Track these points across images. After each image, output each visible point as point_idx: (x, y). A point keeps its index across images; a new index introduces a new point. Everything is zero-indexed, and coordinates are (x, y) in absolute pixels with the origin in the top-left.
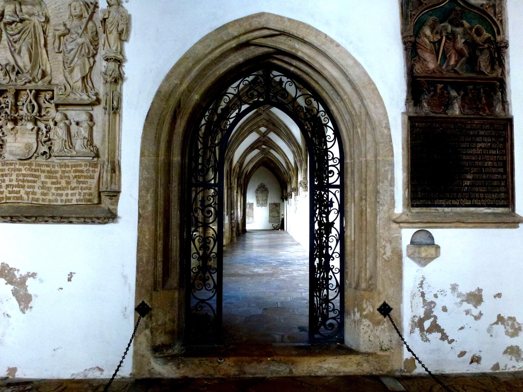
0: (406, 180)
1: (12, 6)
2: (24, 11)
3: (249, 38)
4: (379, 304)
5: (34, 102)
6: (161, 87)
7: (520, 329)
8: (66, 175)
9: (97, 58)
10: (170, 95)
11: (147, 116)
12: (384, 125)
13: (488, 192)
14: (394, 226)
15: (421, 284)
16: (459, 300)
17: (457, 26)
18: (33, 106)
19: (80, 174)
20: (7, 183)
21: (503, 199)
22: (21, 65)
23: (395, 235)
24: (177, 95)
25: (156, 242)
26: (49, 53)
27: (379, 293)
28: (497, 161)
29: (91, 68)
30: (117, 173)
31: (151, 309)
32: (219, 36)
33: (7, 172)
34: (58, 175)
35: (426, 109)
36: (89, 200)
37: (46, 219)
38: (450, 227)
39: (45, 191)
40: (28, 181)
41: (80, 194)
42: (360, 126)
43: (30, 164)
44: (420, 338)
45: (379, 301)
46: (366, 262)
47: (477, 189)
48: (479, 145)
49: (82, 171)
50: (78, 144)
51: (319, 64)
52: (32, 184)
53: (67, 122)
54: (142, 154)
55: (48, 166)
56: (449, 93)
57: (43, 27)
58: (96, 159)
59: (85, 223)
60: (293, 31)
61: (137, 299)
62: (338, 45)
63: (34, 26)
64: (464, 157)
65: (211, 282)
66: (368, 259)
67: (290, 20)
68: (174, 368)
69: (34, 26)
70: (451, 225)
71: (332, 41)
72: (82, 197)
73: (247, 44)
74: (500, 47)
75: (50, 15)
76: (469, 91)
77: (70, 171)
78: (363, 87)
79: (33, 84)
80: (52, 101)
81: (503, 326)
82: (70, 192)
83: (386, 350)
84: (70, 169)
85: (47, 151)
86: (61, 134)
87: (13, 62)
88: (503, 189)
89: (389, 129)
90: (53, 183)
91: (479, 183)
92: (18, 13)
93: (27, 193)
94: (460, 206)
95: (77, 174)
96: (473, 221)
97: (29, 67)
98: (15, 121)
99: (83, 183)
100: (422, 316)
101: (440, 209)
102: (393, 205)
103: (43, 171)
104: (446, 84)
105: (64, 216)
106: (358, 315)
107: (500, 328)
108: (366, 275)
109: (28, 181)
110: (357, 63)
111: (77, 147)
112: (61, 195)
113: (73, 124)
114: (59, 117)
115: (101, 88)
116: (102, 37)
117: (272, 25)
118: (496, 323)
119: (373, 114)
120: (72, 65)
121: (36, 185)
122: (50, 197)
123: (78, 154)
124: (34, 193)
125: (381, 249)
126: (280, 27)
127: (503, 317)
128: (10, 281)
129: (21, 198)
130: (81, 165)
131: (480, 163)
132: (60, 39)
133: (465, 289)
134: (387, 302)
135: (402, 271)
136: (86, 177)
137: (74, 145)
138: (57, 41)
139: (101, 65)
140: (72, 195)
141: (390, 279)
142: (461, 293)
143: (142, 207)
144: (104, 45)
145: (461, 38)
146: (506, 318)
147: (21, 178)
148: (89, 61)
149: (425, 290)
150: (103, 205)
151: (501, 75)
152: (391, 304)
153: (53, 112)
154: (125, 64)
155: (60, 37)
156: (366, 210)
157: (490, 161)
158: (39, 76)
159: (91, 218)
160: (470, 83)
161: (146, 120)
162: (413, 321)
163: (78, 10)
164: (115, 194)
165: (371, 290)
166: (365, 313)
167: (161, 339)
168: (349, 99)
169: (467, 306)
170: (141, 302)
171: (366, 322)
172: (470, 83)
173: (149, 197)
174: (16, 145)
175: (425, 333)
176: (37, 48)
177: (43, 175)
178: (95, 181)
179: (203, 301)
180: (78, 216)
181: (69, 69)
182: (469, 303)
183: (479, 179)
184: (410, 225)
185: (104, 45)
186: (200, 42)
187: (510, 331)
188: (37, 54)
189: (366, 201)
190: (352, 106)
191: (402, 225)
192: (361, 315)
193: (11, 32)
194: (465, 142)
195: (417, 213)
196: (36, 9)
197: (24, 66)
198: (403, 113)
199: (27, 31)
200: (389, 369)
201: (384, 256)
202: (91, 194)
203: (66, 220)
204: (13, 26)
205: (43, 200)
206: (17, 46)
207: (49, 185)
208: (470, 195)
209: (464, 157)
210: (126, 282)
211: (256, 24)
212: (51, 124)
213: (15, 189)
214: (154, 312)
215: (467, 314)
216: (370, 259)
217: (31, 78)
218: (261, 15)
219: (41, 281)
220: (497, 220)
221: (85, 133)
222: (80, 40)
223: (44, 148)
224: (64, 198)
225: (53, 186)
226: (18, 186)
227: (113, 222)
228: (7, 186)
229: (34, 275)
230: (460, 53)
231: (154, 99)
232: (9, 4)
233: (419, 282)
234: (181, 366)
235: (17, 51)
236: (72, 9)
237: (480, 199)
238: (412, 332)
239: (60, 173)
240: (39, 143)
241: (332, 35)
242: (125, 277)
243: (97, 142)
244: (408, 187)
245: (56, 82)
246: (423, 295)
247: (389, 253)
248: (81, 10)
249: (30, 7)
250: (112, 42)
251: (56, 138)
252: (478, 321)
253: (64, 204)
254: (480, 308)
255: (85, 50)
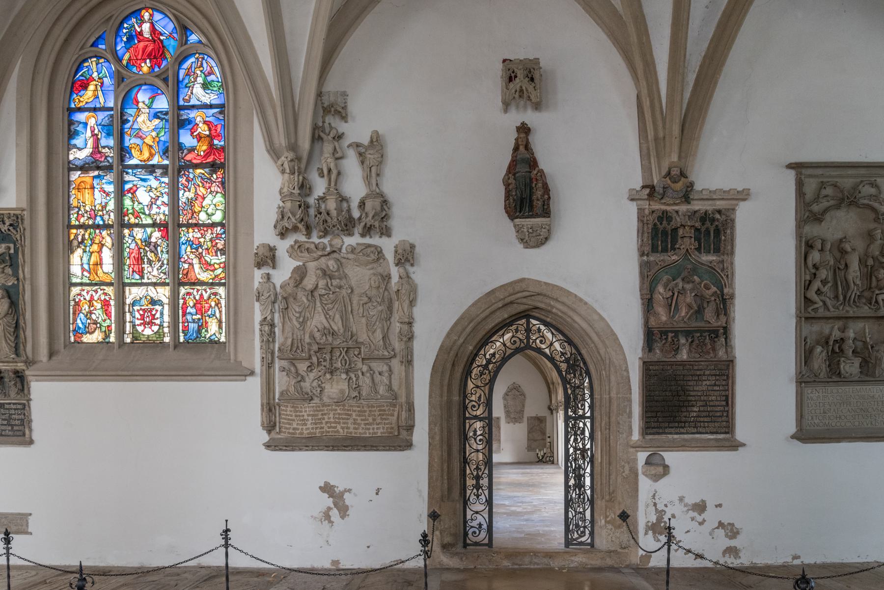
0: (641, 413)
1: (325, 281)
2: (334, 284)
3: (512, 299)
4: (618, 512)
5: (346, 357)
6: (443, 342)
7: (738, 533)
8: (372, 413)
9: (392, 320)
10: (451, 349)
11: (433, 366)
12: (624, 369)
13: (711, 422)
14: (632, 450)
15: (654, 495)
16: (686, 509)
17: (688, 282)
18: (346, 360)
19: (383, 413)
20: (327, 420)
21: (725, 427)
22: (336, 328)
23: (632, 457)
24: (455, 348)
25: (442, 464)
26: (354, 317)
27: (619, 503)
28: (720, 396)
29: (388, 328)
30: (412, 411)
31: (439, 516)
32: (488, 299)
33: (326, 412)
34: (367, 414)
35: (658, 355)
36: (391, 433)
37: (359, 448)
38: (679, 451)
39: (357, 426)
40: (343, 419)
41: (383, 428)
42: (605, 369)
43: (344, 405)
44: (653, 539)
45: (619, 509)
46: (609, 479)
47: (702, 419)
48: (704, 383)
49: (384, 410)
50: (382, 390)
51: (571, 318)
52: (346, 421)
53: (371, 372)
54: (430, 396)
55: (358, 407)
56: (678, 340)
57: (349, 296)
58: (394, 401)
59: (389, 450)
60: (549, 293)
61: (429, 508)
62: (586, 303)
63: (343, 297)
64: (692, 393)
65: (483, 497)
66: (611, 477)
67: (546, 283)
68: (458, 560)
69: (343, 297)
70: (679, 449)
71: (581, 300)
72: (385, 431)
73: (512, 303)
74: (726, 299)
75: (354, 285)
76: (696, 338)
77: (375, 411)
78: (607, 338)
79: (345, 343)
80: (360, 356)
81: (723, 530)
82: (375, 426)
83: (625, 548)
84: (375, 409)
85: (358, 395)
86: (368, 383)
87: (327, 325)
88: (724, 418)
89: (628, 372)
90: (362, 420)
91: (704, 414)
92: (329, 285)
93: (343, 428)
94: (687, 433)
95: (381, 413)
96: (695, 446)
97: (342, 331)
98: (331, 373)
99: (385, 419)
100: (655, 522)
101: (670, 436)
102: (630, 432)
103: (355, 411)
104: (676, 333)
105: (374, 445)
106: (603, 522)
107: (721, 532)
108: (609, 489)
109: (343, 419)
110: (602, 318)
111: (381, 392)
112: (369, 429)
113: (377, 373)
114: (365, 368)
115: (397, 345)
116: (396, 305)
117: (531, 289)
118: (717, 528)
119: (614, 360)
120: (375, 327)
121: (350, 421)
122: (360, 431)
123: (383, 398)
124: (348, 428)
125: (620, 469)
126: (537, 290)
127: (723, 523)
128: (331, 496)
129: (338, 432)
130: (384, 406)
131: (705, 398)
132: (363, 306)
133: (691, 500)
134: (625, 510)
135: (638, 486)
136: (387, 415)
137: (378, 390)
138: (361, 308)
139: (396, 327)
140: (377, 429)
141: (628, 492)
142: (687, 504)
143: (431, 437)
144: (398, 310)
145: (691, 293)
146: (726, 524)
147: (337, 416)
148: (387, 324)
149: (657, 501)
150: (401, 437)
151: (726, 323)
152: (629, 512)
153: (359, 364)
154: (414, 324)
155: (363, 304)
156: (609, 437)
157: (713, 396)
158: (350, 337)
159: (394, 446)
160: (696, 331)
161: (432, 369)
162: (647, 526)
163: (377, 283)
164: (410, 428)
165: (613, 501)
166: (608, 519)
167: (448, 539)
168: (596, 347)
169: (692, 514)
170: (432, 510)
171: (609, 527)
172: (696, 331)
173: (437, 429)
174: (332, 390)
175: (657, 535)
176: (346, 314)
177: (354, 414)
178: (395, 418)
179: (477, 513)
180: (384, 445)
181: (370, 327)
182: (694, 512)
183: (704, 411)
184: (643, 449)
185: (398, 310)
186: (474, 305)
187: (729, 534)
188: (346, 319)
189: (609, 430)
190: (599, 353)
191: (638, 449)
192: (606, 522)
193: (325, 302)
194: (692, 380)
195: (650, 439)
196: (344, 281)
197: (339, 330)
198: (640, 358)
199: (339, 302)
200: (628, 563)
201: (623, 474)
202: (392, 428)
203: (375, 448)
204: (326, 296)
205: (356, 433)
206: (331, 313)
207: (359, 421)
208: (695, 424)
209: (692, 393)
210: (420, 496)
211: (517, 288)
212: (360, 374)
213: (332, 425)
214: (442, 518)
215: (692, 520)
216: (613, 477)
217: (345, 340)
218: (522, 280)
219: (355, 495)
220: (717, 445)
221: (386, 381)
222: (380, 308)
223: (356, 394)
224: (371, 431)
225: (363, 422)
226: (335, 423)
227: (410, 450)
228: (327, 423)
229: (349, 491)
230: (690, 306)
231: (438, 352)
232: (323, 279)
233: (652, 494)
234: (464, 558)
235: (332, 317)
236: (373, 283)
237: (705, 427)
238: (646, 534)
239: (368, 412)
240: (350, 388)
241: (581, 295)
242: (420, 491)
243: (395, 387)
244: (643, 419)
245: (361, 340)
246: (655, 505)
247: (627, 472)
248: (379, 282)
249: (338, 281)
250: (406, 310)
251: (364, 385)
252: (702, 526)
253: (371, 436)
254: (703, 516)
255: (384, 315)
